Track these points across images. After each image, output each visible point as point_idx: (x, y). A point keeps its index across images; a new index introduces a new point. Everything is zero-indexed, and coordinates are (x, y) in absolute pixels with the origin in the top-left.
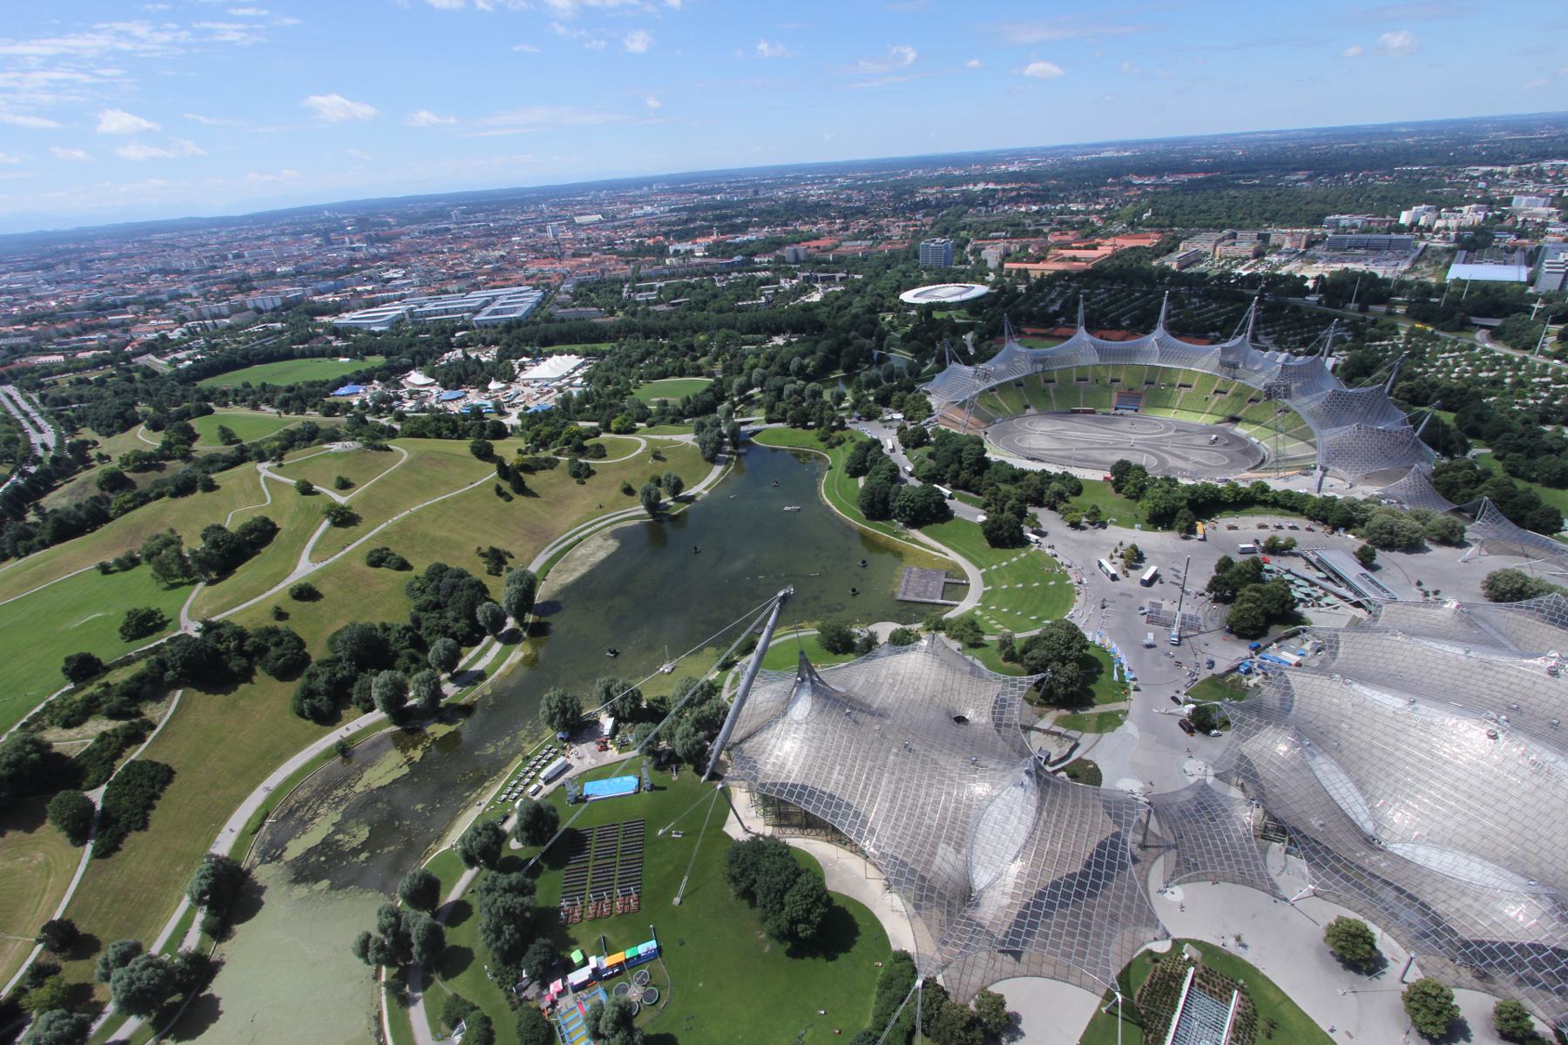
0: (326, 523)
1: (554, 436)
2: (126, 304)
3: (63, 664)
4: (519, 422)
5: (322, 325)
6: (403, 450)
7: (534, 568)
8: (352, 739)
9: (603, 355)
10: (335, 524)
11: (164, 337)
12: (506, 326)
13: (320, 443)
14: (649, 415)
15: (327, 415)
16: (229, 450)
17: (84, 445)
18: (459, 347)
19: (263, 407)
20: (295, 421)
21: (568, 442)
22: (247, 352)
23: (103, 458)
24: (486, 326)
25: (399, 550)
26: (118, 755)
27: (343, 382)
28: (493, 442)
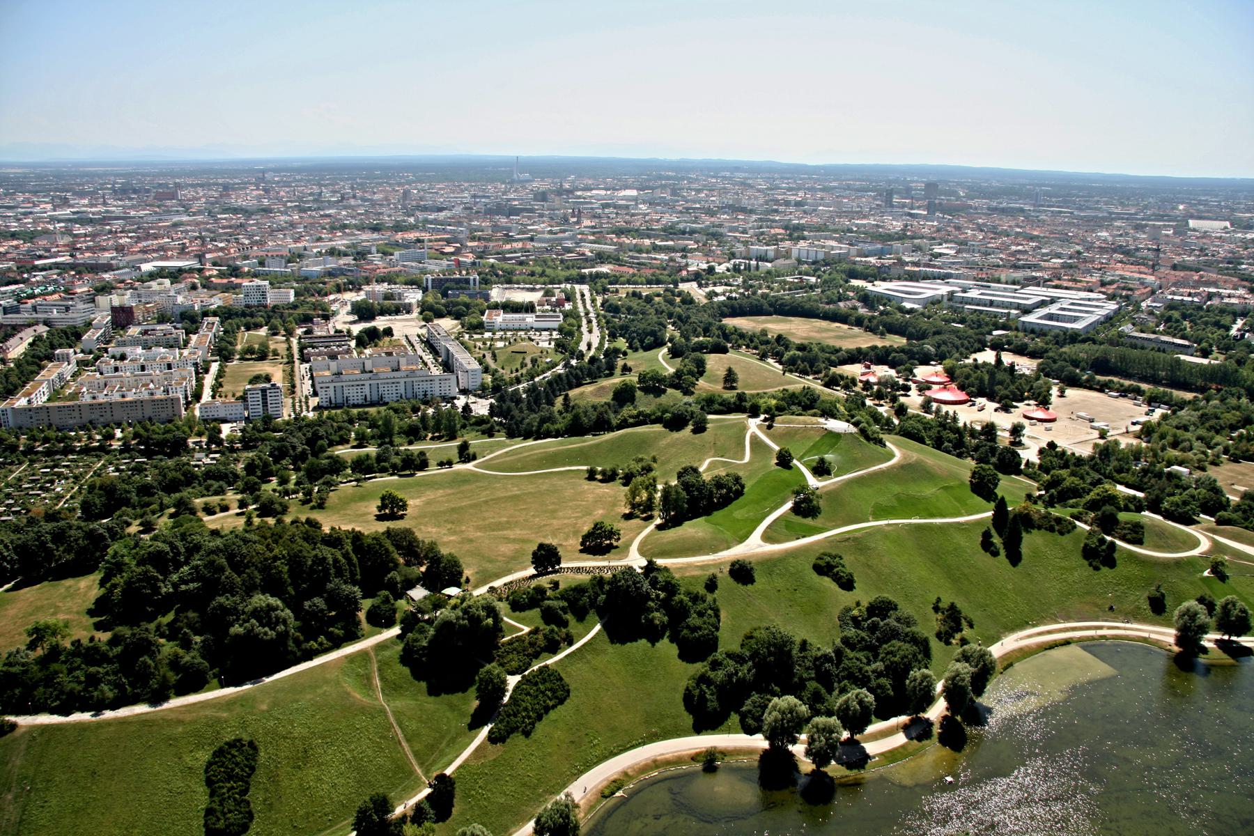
0: (789, 505)
1: (1075, 493)
2: (692, 232)
3: (536, 548)
4: (1035, 460)
5: (854, 289)
6: (898, 451)
7: (997, 651)
8: (724, 753)
9: (1182, 405)
10: (796, 509)
11: (711, 270)
12: (1057, 336)
13: (814, 415)
14: (1224, 505)
15: (827, 385)
16: (730, 395)
17: (616, 352)
18: (993, 348)
19: (770, 361)
20: (798, 383)
21: (1093, 505)
22: (777, 299)
23: (626, 369)
24: (1033, 331)
25: (850, 563)
26: (536, 656)
27: (854, 357)
28: (1000, 476)
